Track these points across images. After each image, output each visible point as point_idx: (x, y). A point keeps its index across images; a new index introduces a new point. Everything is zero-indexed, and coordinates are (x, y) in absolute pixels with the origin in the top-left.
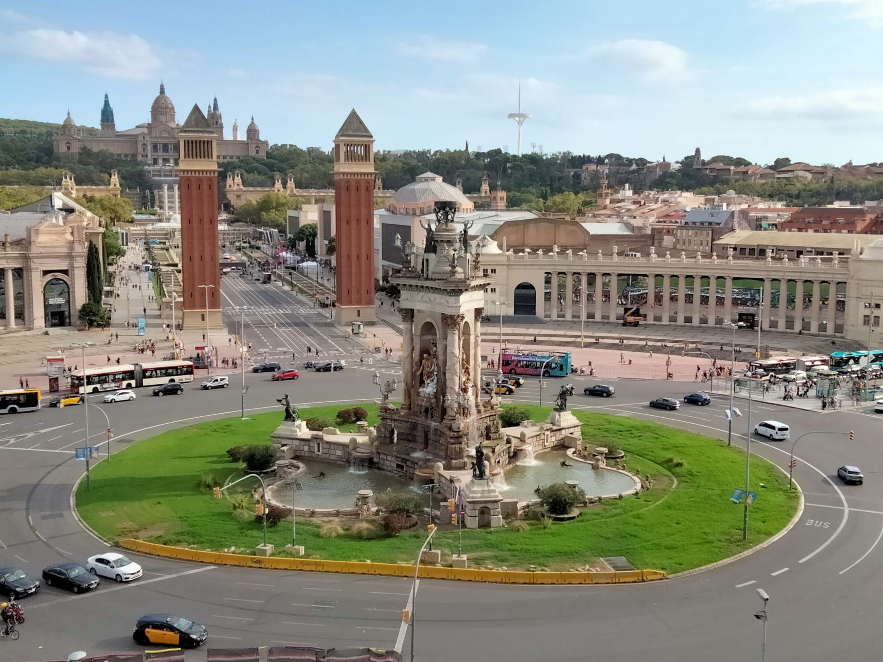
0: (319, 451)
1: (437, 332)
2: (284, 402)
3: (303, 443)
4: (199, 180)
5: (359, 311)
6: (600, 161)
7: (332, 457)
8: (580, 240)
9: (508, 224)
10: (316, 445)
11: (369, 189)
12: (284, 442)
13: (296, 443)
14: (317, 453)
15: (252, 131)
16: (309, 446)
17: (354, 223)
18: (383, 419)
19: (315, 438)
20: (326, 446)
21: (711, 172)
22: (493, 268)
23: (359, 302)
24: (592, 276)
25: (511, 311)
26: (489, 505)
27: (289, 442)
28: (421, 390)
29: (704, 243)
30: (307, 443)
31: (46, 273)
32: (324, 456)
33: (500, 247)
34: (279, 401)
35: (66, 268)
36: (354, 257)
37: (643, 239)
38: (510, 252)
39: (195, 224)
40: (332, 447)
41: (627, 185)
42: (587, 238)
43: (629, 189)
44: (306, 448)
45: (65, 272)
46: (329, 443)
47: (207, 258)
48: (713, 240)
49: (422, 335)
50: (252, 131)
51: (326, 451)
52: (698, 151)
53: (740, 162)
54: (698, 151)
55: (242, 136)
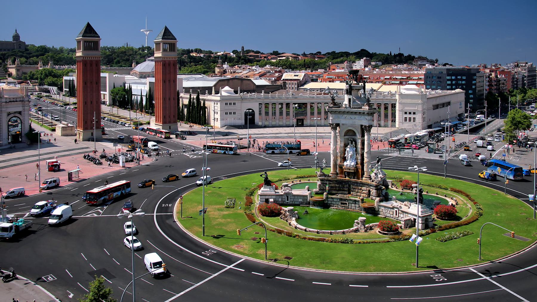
0: (288, 200)
1: (357, 134)
2: (264, 176)
3: (278, 197)
4: (91, 61)
5: (170, 127)
6: (197, 51)
7: (296, 203)
8: (252, 87)
9: (220, 81)
10: (286, 197)
11: (175, 65)
12: (267, 197)
13: (274, 197)
14: (286, 201)
15: (16, 37)
16: (282, 198)
17: (167, 82)
18: (321, 180)
19: (286, 194)
20: (292, 197)
21: (250, 57)
22: (234, 102)
23: (170, 122)
24: (288, 105)
25: (242, 122)
26: (428, 217)
27: (269, 197)
28: (345, 163)
29: (294, 88)
30: (281, 197)
31: (9, 114)
32: (291, 203)
33: (236, 92)
34: (261, 176)
35: (20, 110)
36: (168, 99)
37: (278, 87)
38: (241, 94)
39: (89, 84)
40: (296, 197)
41: (226, 62)
42: (255, 87)
43: (227, 64)
44: (280, 200)
45: (20, 113)
46: (295, 196)
47: (95, 103)
48: (298, 87)
49: (344, 136)
50: (16, 37)
51: (292, 200)
52: (243, 47)
53: (258, 52)
54: (243, 47)
55: (11, 39)
